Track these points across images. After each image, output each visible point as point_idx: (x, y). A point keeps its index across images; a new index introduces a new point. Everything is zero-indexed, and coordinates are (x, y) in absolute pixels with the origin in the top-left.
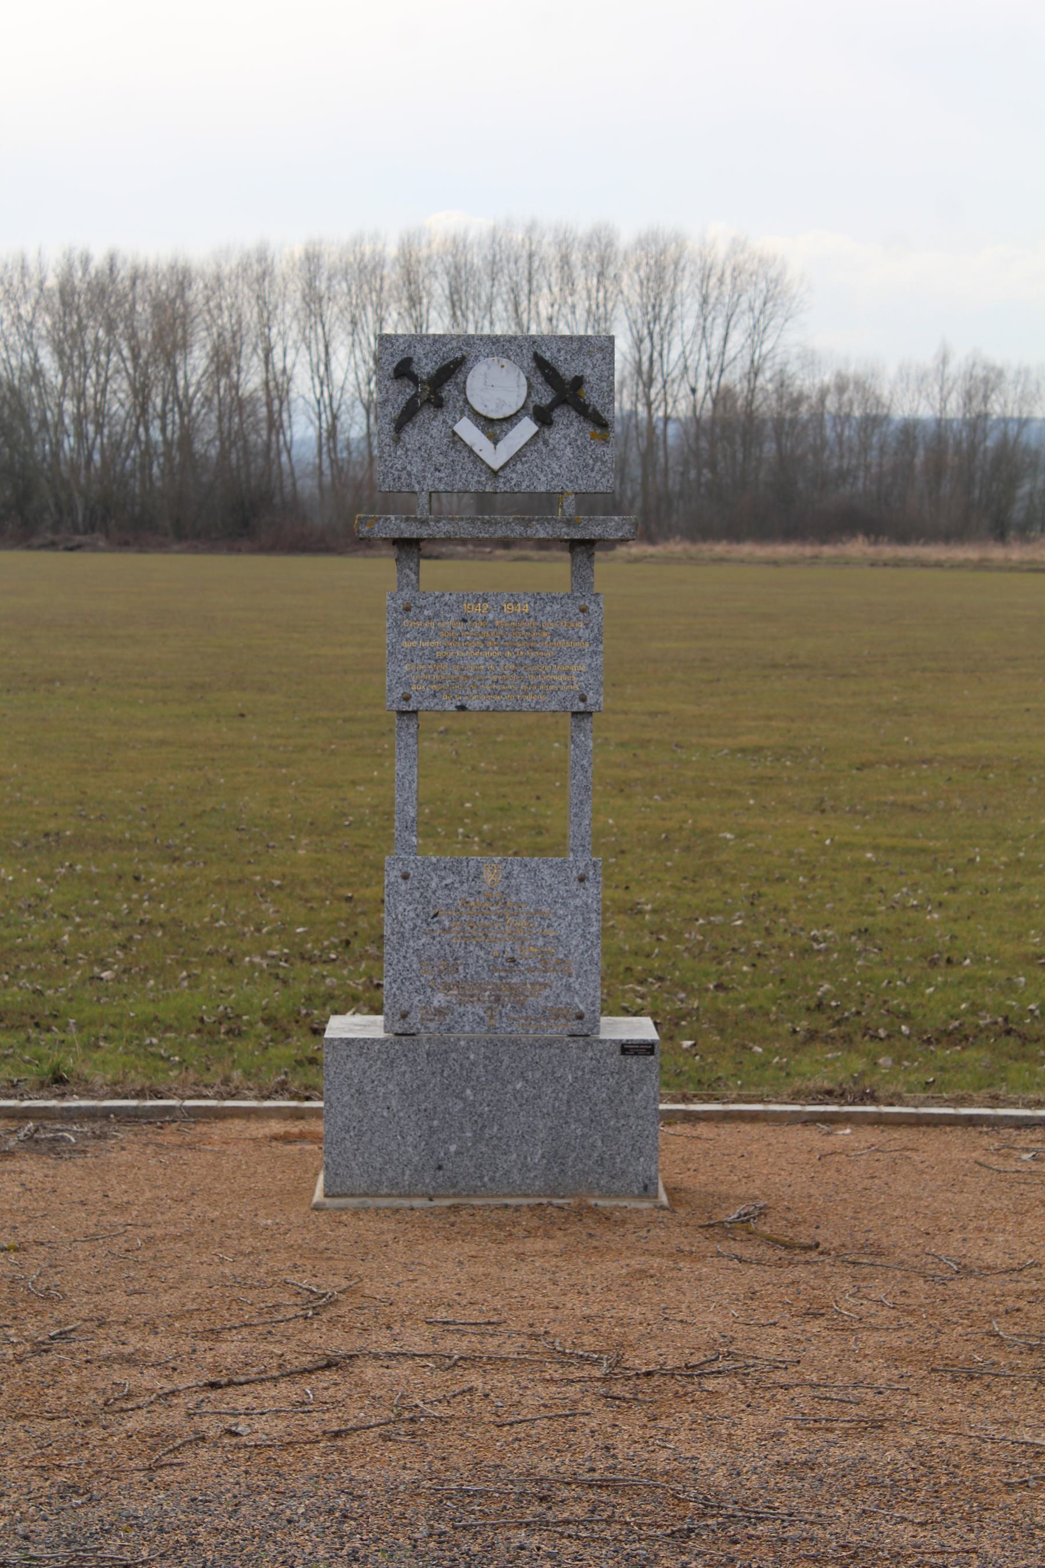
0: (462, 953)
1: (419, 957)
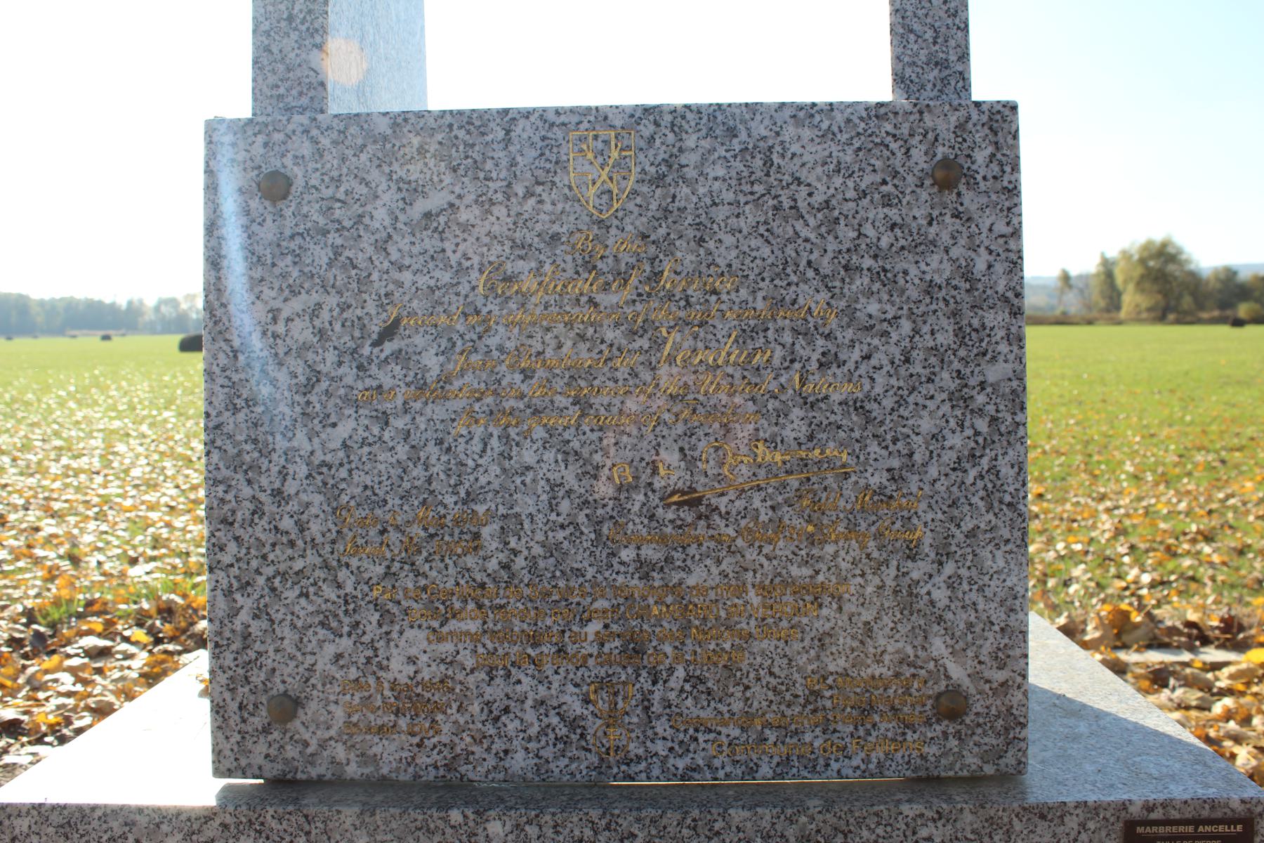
0: (491, 474)
1: (331, 491)
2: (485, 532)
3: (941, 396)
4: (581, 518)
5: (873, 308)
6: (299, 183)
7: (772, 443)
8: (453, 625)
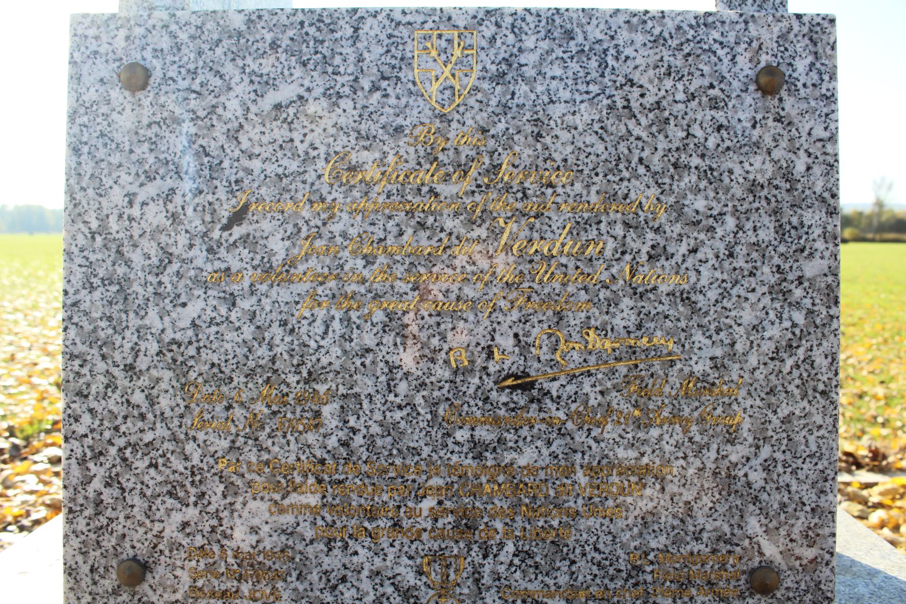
0: (333, 356)
1: (180, 367)
2: (326, 410)
3: (761, 290)
4: (418, 400)
5: (700, 204)
6: (157, 75)
7: (603, 330)
8: (294, 498)
